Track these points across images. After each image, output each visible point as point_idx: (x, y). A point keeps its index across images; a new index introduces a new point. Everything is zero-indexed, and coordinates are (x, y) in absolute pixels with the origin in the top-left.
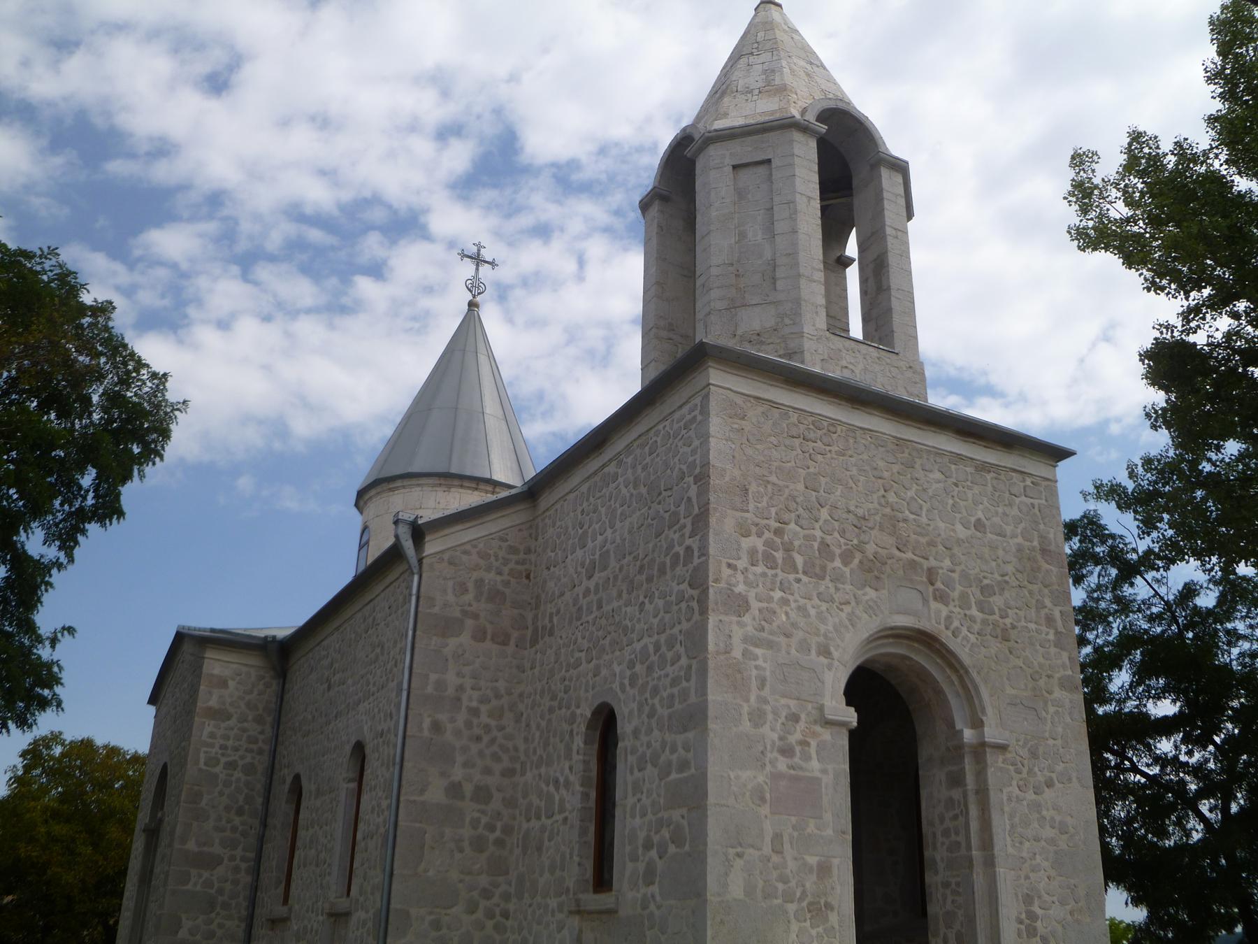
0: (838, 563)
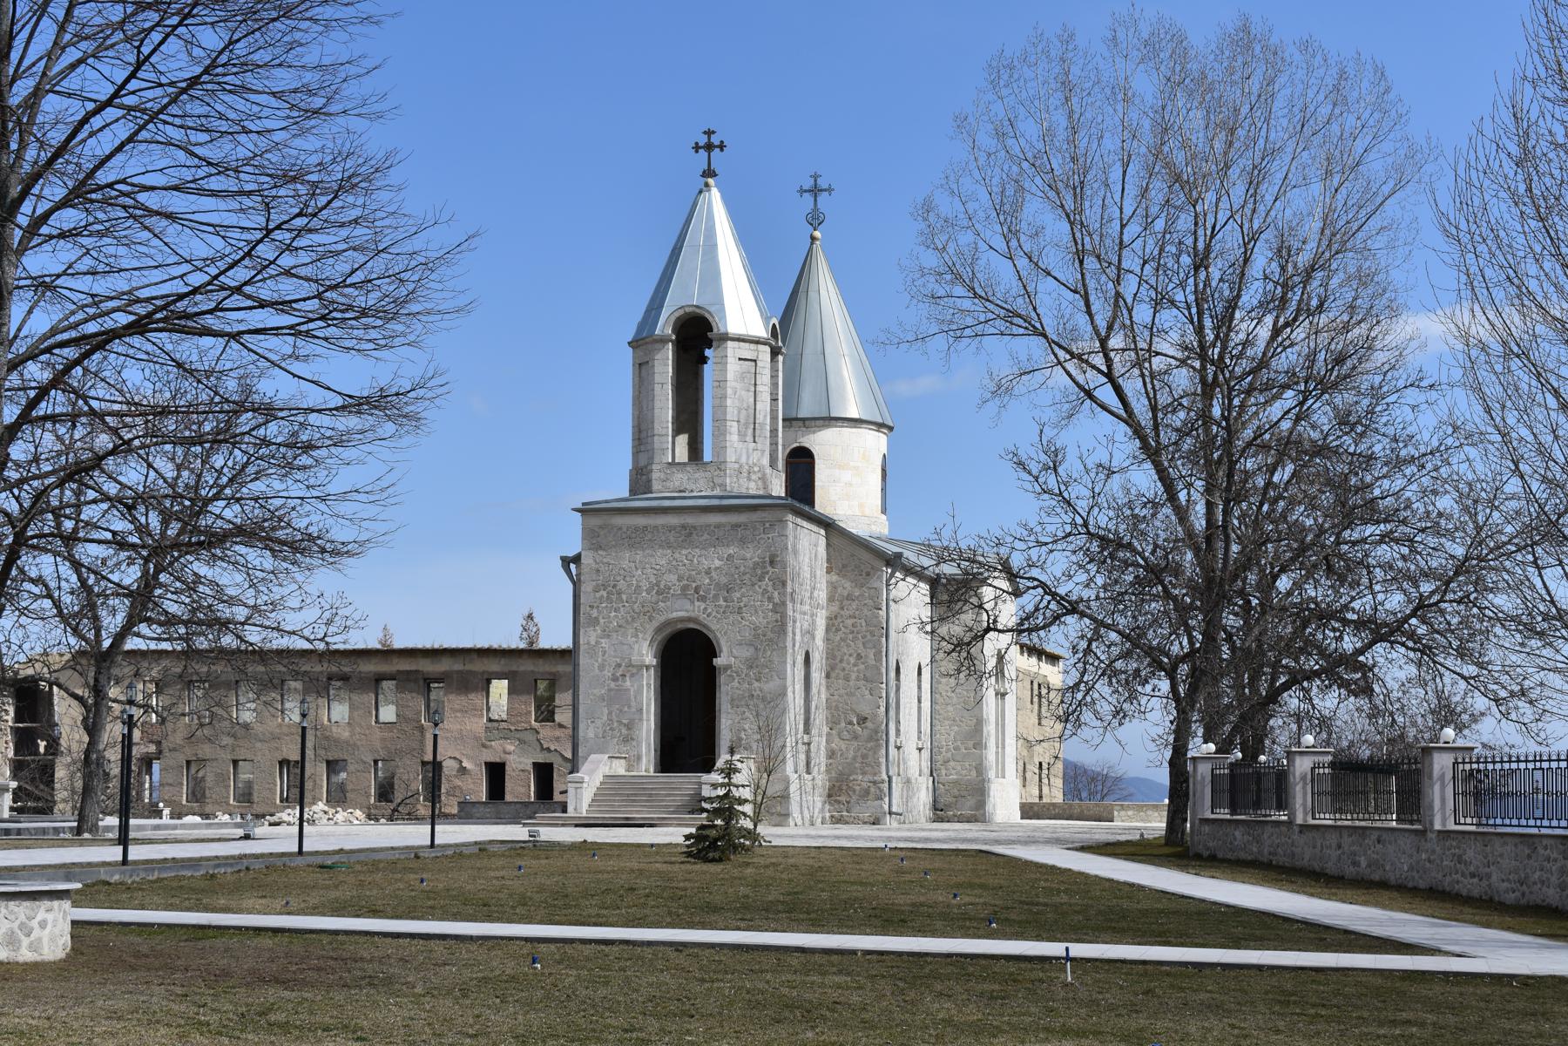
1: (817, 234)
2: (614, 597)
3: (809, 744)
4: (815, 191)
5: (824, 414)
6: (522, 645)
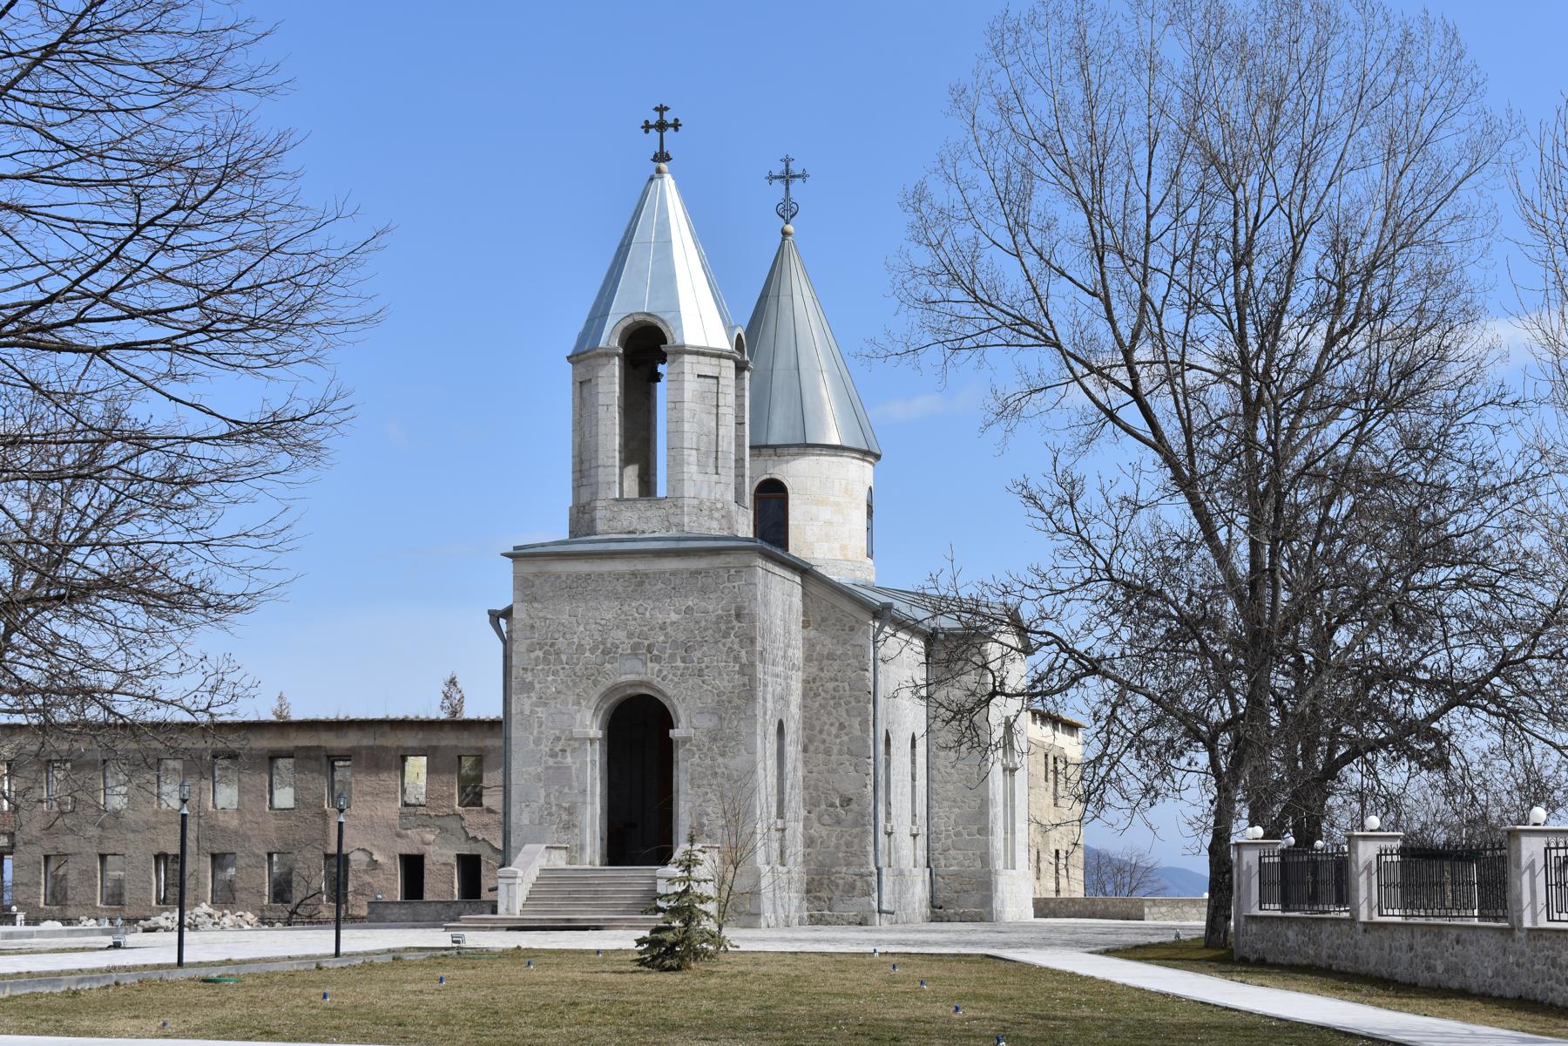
0: (587, 654)
1: (790, 228)
2: (552, 658)
3: (783, 830)
4: (787, 177)
5: (799, 441)
6: (443, 716)
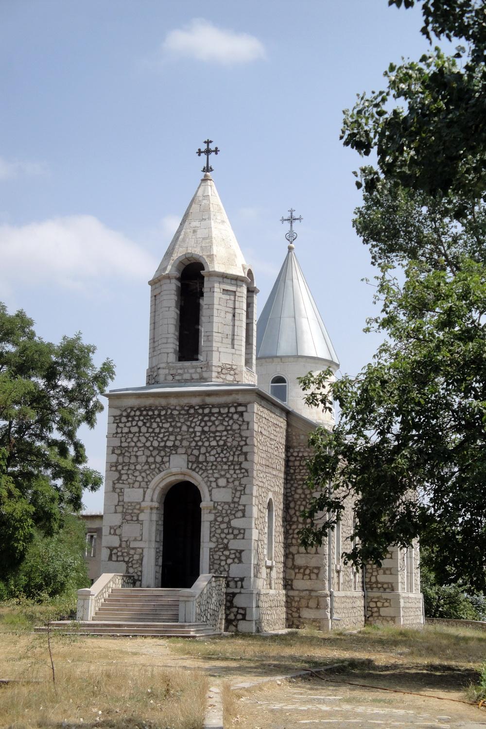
1: (293, 245)
5: (294, 354)
